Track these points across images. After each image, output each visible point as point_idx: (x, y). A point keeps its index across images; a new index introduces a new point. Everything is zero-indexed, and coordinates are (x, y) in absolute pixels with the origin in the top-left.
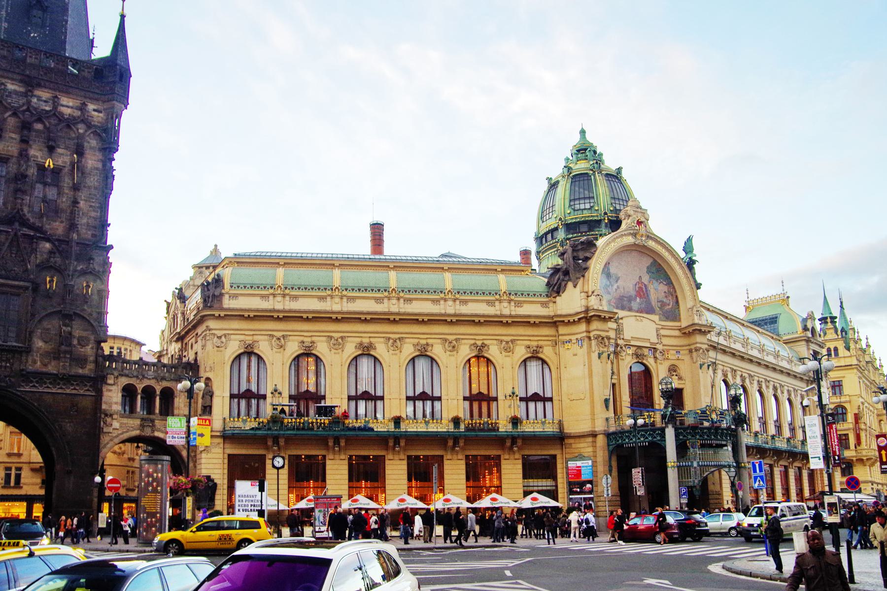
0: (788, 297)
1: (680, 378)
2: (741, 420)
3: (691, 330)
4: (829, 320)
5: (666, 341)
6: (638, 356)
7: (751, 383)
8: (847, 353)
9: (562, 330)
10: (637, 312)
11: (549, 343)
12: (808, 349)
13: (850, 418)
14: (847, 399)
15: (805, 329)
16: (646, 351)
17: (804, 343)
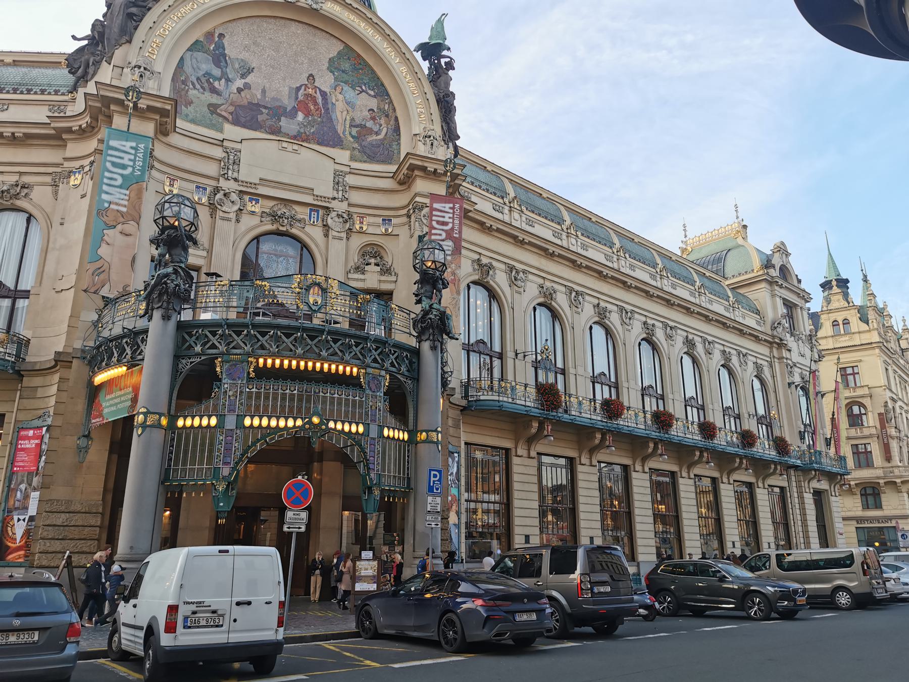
0: (745, 227)
1: (386, 271)
2: (435, 327)
3: (405, 171)
4: (834, 283)
5: (356, 197)
6: (275, 217)
7: (623, 323)
8: (864, 327)
9: (75, 149)
10: (295, 137)
11: (48, 179)
12: (773, 296)
13: (871, 420)
14: (866, 391)
15: (768, 264)
16: (302, 213)
17: (763, 285)
